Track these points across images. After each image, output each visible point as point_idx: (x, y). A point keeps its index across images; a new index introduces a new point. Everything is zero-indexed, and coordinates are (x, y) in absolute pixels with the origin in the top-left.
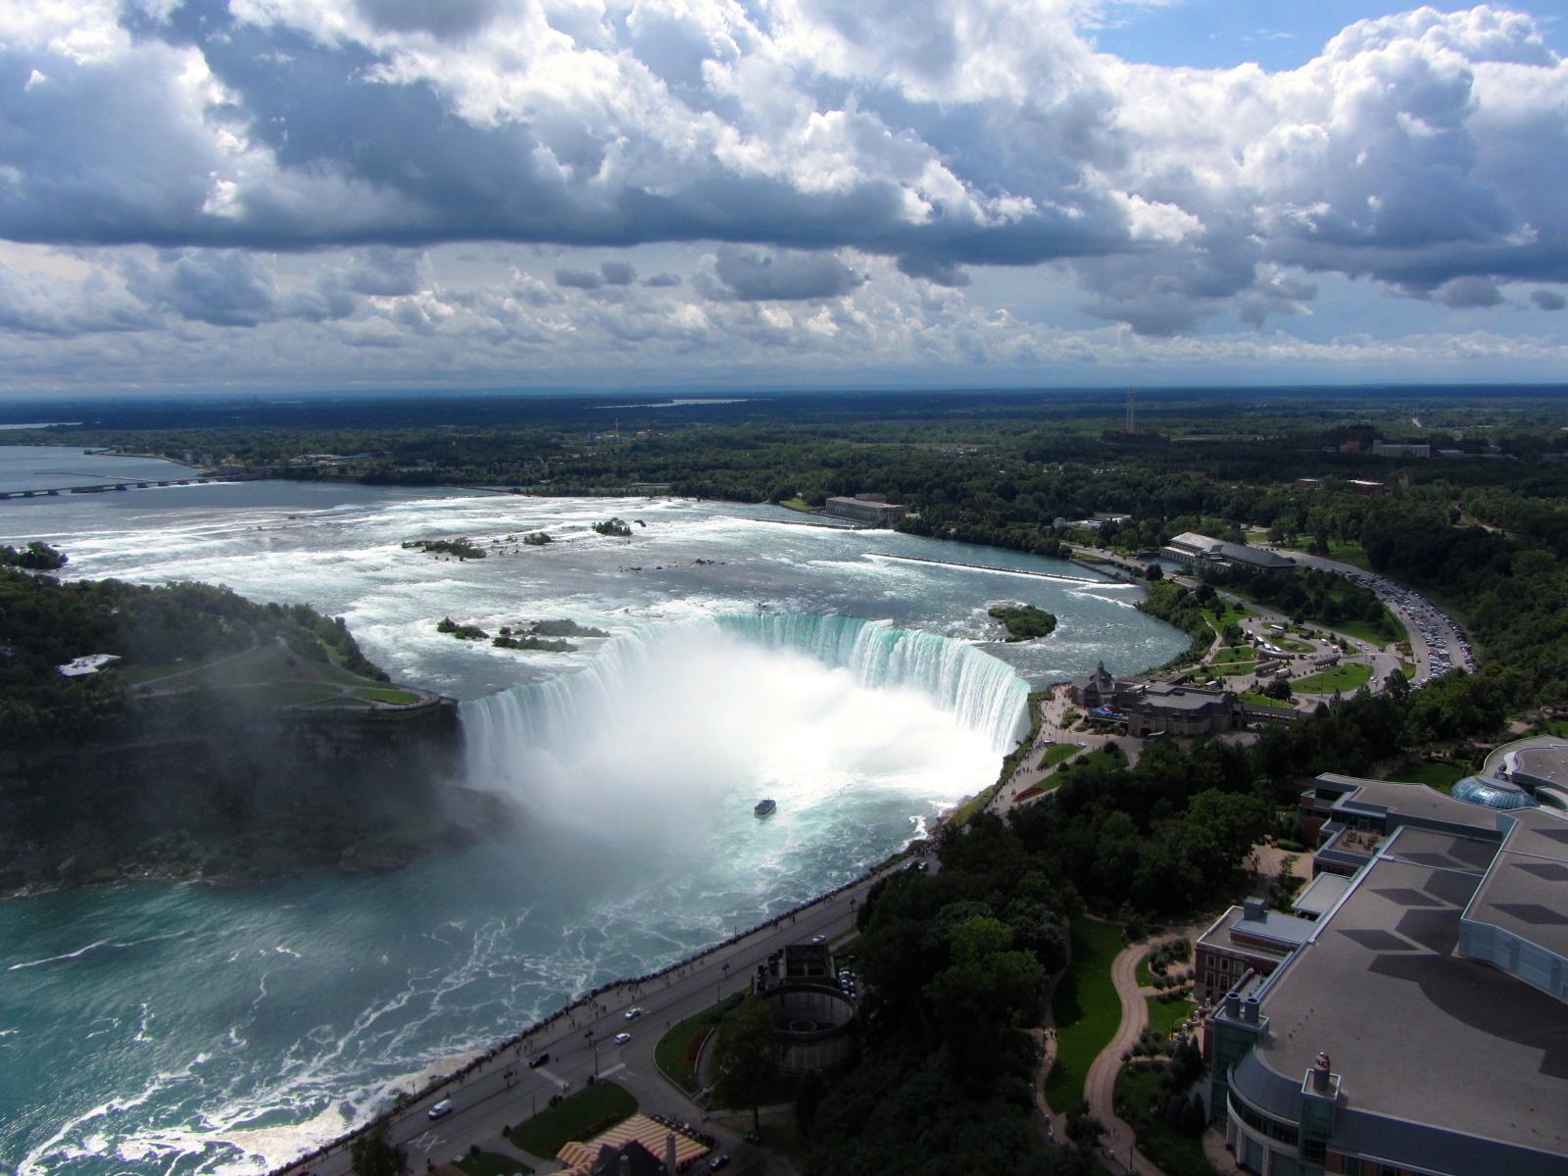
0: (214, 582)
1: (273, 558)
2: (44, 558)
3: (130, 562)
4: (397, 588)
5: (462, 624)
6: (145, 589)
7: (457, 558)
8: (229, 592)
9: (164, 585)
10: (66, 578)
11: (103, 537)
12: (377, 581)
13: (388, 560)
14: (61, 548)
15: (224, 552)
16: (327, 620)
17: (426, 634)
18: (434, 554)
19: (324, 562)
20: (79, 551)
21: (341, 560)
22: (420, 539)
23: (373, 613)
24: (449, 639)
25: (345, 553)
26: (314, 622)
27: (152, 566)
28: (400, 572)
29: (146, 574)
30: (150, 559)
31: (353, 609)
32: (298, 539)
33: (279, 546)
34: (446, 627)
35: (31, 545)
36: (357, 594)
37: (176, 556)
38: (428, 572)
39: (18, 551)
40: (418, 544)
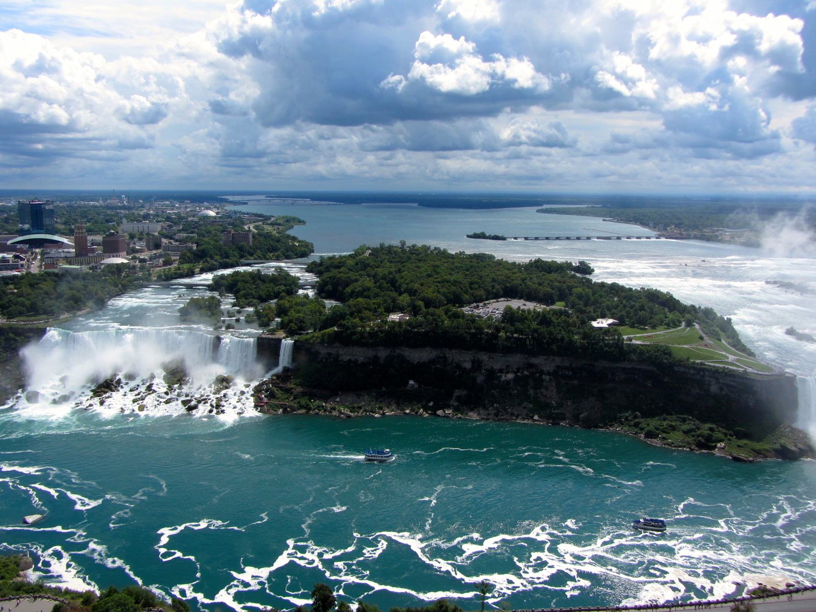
0: (664, 290)
1: (693, 281)
2: (585, 269)
3: (621, 275)
4: (760, 306)
5: (801, 332)
6: (630, 289)
7: (799, 293)
8: (671, 297)
9: (639, 289)
10: (594, 280)
11: (610, 262)
12: (749, 301)
13: (757, 289)
14: (592, 265)
15: (668, 276)
16: (722, 318)
17: (778, 333)
18: (784, 289)
19: (719, 287)
20: (599, 267)
21: (729, 286)
22: (777, 280)
23: (746, 318)
24: (791, 339)
25: (732, 283)
26: (714, 318)
27: (632, 278)
28: (763, 297)
29: (630, 282)
30: (631, 275)
31: (735, 314)
32: (706, 272)
33: (695, 275)
34: (790, 332)
35: (580, 262)
36: (738, 306)
37: (643, 275)
38: (782, 300)
39: (574, 264)
40: (775, 283)
